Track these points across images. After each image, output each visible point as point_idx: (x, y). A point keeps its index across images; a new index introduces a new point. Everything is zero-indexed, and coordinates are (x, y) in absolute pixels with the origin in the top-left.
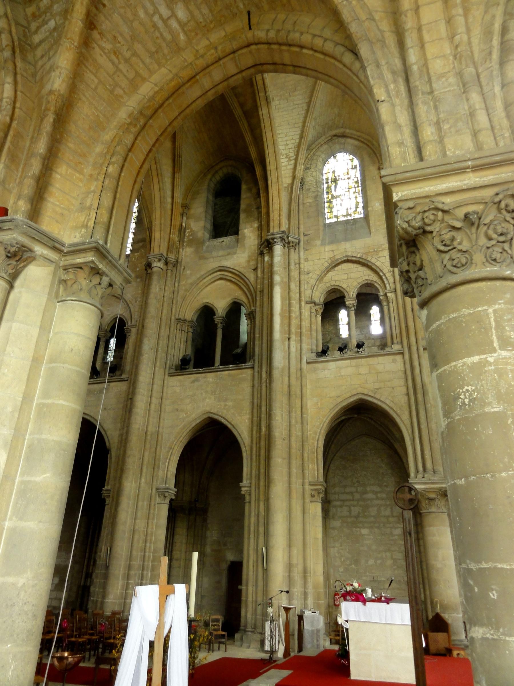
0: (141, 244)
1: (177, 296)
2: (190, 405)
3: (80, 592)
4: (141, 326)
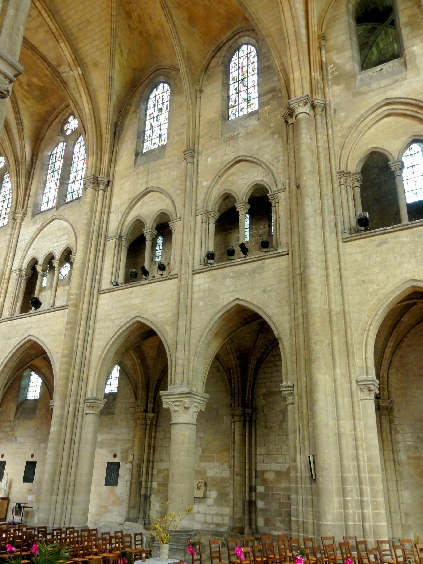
0: (270, 95)
1: (333, 145)
2: (382, 274)
3: (246, 508)
4: (294, 188)
